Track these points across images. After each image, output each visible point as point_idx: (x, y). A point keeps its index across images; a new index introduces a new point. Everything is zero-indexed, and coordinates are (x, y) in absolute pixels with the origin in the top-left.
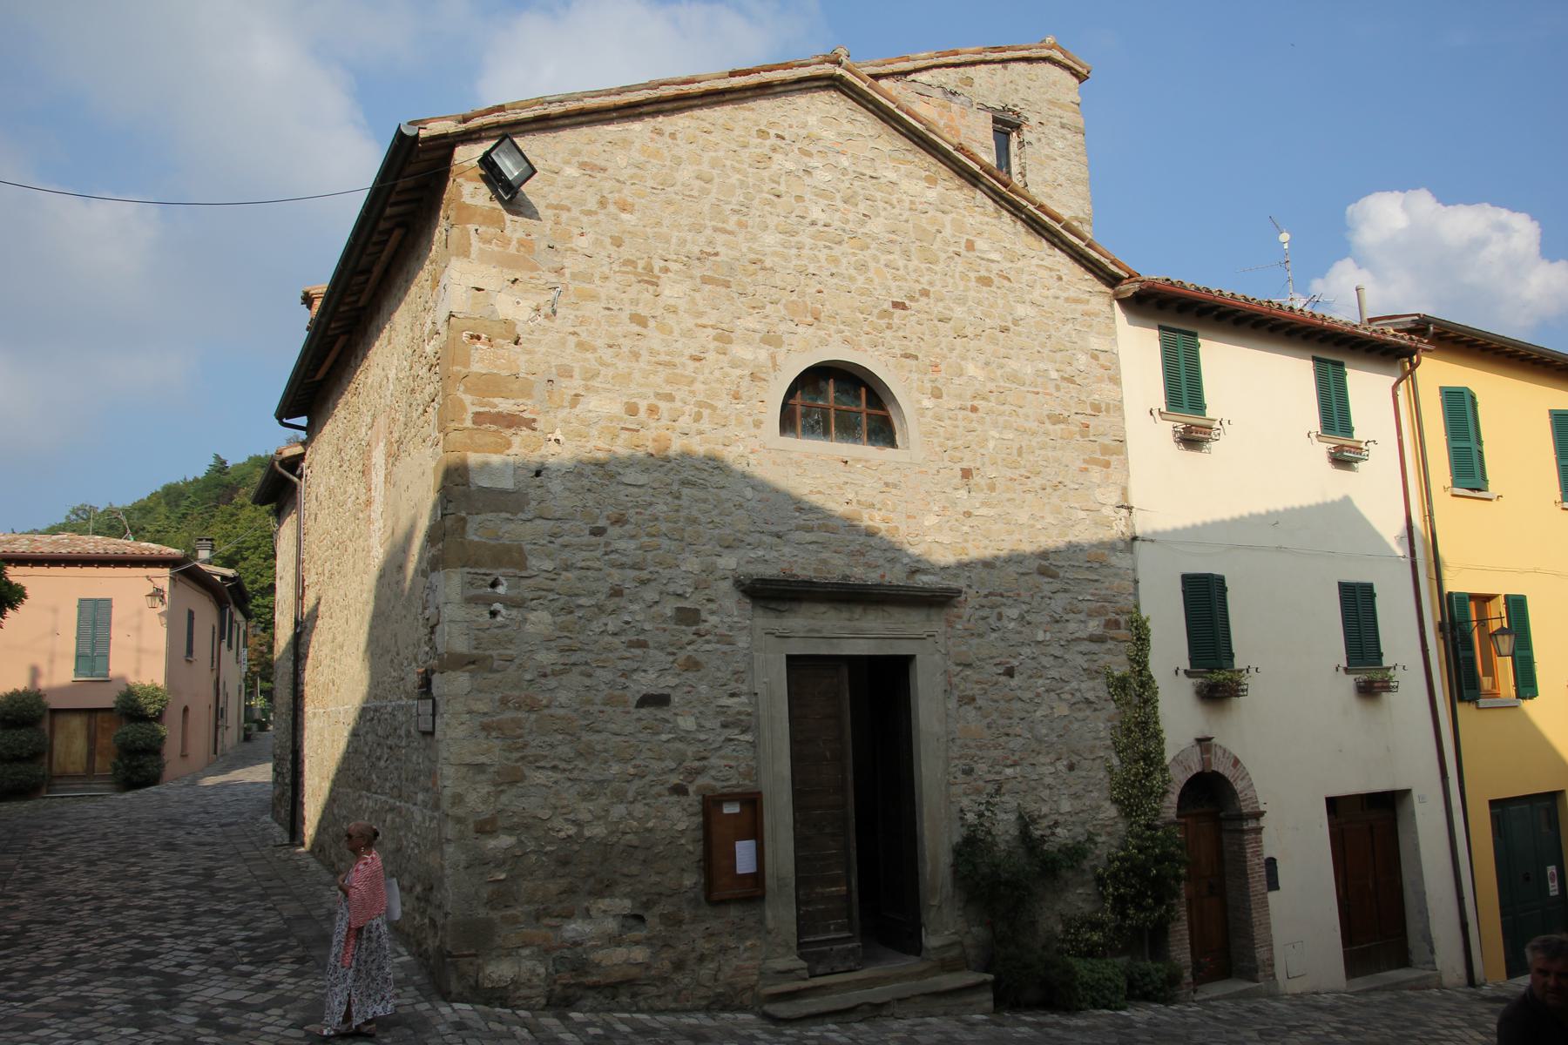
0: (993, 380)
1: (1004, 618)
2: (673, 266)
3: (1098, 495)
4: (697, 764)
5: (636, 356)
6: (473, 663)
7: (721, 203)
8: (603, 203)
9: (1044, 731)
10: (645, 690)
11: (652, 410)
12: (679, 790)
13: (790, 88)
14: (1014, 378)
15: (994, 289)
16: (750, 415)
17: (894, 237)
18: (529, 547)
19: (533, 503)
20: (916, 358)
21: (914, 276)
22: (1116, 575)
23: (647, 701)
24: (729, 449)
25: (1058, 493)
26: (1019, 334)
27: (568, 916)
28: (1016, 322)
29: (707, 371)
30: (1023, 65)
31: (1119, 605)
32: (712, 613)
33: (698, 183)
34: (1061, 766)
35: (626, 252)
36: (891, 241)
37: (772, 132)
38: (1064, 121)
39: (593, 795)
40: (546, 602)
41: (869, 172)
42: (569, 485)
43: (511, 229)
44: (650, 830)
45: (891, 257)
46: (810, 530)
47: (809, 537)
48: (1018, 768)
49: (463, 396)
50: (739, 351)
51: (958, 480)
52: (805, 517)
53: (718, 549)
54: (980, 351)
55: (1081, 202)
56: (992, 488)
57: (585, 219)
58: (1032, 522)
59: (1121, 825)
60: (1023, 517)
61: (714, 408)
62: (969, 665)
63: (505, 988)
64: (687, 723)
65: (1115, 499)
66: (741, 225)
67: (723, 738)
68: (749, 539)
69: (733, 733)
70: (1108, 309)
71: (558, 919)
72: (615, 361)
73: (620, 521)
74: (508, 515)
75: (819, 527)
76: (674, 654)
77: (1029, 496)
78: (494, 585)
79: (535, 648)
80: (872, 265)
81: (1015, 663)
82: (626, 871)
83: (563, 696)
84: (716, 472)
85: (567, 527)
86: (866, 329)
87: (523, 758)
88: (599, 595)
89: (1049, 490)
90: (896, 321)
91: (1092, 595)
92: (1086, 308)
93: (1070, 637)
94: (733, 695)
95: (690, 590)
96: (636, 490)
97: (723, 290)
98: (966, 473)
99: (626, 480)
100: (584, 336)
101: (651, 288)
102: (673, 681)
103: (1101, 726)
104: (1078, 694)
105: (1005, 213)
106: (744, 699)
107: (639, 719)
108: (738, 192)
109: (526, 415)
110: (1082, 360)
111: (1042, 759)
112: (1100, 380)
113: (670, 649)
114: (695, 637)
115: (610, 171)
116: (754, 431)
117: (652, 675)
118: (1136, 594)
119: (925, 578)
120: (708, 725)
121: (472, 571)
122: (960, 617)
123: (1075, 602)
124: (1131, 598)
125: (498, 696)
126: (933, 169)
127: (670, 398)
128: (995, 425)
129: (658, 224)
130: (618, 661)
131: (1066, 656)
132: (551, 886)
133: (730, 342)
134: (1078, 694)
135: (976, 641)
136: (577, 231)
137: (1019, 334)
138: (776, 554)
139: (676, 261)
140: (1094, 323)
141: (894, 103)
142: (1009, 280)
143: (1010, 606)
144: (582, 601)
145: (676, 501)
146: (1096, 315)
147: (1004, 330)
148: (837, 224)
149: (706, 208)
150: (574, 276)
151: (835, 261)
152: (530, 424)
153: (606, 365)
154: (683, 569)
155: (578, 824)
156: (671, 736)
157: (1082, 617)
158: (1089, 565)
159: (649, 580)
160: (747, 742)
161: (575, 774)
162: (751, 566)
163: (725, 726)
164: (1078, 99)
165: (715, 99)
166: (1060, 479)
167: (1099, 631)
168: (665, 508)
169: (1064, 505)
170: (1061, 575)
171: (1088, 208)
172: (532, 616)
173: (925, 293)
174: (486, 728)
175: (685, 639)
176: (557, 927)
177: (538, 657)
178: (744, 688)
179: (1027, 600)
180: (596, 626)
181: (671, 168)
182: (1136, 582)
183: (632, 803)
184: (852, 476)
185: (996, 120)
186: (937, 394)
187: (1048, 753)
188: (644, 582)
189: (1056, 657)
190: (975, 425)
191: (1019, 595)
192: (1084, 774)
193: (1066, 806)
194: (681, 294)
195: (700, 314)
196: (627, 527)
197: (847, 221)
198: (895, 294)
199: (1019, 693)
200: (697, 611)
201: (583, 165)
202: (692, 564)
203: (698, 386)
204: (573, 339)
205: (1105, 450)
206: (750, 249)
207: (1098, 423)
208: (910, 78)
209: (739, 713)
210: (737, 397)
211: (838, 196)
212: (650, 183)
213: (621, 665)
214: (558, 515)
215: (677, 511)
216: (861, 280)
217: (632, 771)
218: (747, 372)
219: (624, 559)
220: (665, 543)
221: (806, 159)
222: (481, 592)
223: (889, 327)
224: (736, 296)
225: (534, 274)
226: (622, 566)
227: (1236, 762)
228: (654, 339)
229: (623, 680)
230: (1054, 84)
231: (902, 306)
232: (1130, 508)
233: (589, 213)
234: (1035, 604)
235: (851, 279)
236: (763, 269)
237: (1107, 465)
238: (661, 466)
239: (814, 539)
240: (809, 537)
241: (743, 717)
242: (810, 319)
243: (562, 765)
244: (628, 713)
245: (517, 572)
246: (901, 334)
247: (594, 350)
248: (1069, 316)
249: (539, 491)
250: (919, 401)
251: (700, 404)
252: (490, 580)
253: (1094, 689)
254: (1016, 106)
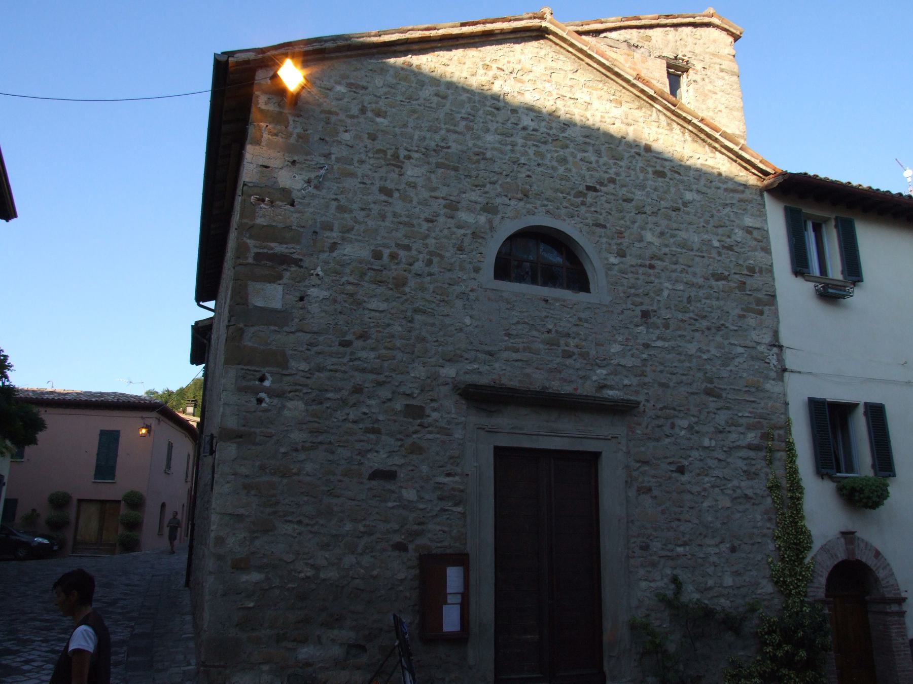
0: (666, 246)
3: (754, 335)
4: (416, 527)
5: (383, 217)
6: (241, 437)
7: (453, 113)
8: (363, 110)
9: (710, 519)
10: (376, 466)
11: (393, 256)
12: (401, 547)
13: (508, 37)
14: (684, 245)
15: (667, 179)
16: (470, 263)
17: (588, 140)
18: (291, 352)
19: (296, 320)
20: (604, 227)
21: (604, 168)
22: (770, 398)
23: (377, 475)
24: (454, 287)
25: (721, 333)
26: (688, 213)
27: (304, 641)
28: (685, 204)
29: (437, 230)
30: (690, 29)
31: (773, 422)
32: (435, 410)
33: (435, 99)
34: (725, 547)
35: (378, 145)
36: (585, 143)
37: (494, 66)
38: (723, 67)
40: (301, 395)
41: (569, 95)
42: (326, 308)
43: (292, 126)
44: (375, 577)
45: (585, 155)
46: (517, 351)
47: (515, 356)
48: (687, 548)
49: (248, 241)
50: (463, 216)
51: (637, 320)
52: (512, 341)
53: (441, 361)
54: (656, 224)
55: (737, 123)
56: (667, 326)
57: (349, 121)
58: (699, 354)
59: (776, 601)
60: (692, 348)
61: (442, 257)
62: (646, 463)
64: (410, 494)
65: (767, 339)
66: (469, 128)
67: (438, 508)
68: (466, 355)
69: (448, 505)
70: (759, 198)
72: (366, 220)
73: (363, 336)
74: (276, 328)
75: (525, 349)
76: (401, 440)
77: (697, 335)
78: (262, 379)
80: (570, 159)
81: (686, 463)
83: (309, 467)
84: (442, 304)
85: (321, 339)
86: (565, 204)
87: (275, 513)
88: (344, 391)
89: (714, 331)
90: (589, 200)
91: (750, 412)
92: (742, 196)
93: (731, 445)
94: (449, 475)
95: (417, 392)
96: (378, 314)
97: (453, 173)
98: (645, 314)
99: (370, 306)
100: (343, 202)
101: (397, 170)
102: (397, 460)
103: (759, 517)
104: (739, 491)
105: (675, 126)
106: (457, 478)
107: (370, 489)
108: (468, 105)
109: (295, 256)
110: (739, 235)
111: (708, 541)
112: (754, 249)
113: (399, 436)
114: (419, 428)
115: (370, 89)
116: (473, 275)
117: (383, 455)
118: (786, 413)
119: (611, 393)
120: (427, 497)
121: (245, 367)
122: (640, 424)
123: (736, 417)
124: (782, 416)
125: (258, 463)
126: (618, 94)
127: (408, 248)
128: (669, 279)
129: (405, 126)
131: (729, 460)
133: (457, 209)
134: (739, 491)
135: (652, 444)
136: (342, 129)
137: (688, 213)
138: (488, 368)
139: (417, 151)
140: (749, 207)
141: (586, 46)
142: (679, 174)
143: (682, 418)
144: (330, 395)
145: (409, 324)
146: (750, 202)
147: (677, 210)
148: (543, 129)
149: (442, 116)
150: (338, 160)
151: (542, 155)
152: (297, 263)
153: (360, 223)
154: (413, 375)
156: (395, 504)
157: (741, 429)
158: (747, 389)
159: (384, 382)
160: (459, 513)
161: (316, 528)
162: (468, 376)
163: (441, 499)
164: (733, 52)
165: (451, 43)
166: (722, 322)
167: (756, 442)
168: (400, 329)
169: (726, 342)
170: (724, 395)
171: (742, 128)
172: (290, 404)
173: (612, 181)
174: (246, 487)
175: (411, 429)
177: (292, 436)
178: (459, 470)
179: (696, 414)
180: (340, 415)
181: (416, 88)
182: (787, 404)
183: (361, 554)
184: (551, 311)
185: (669, 66)
186: (621, 254)
187: (713, 537)
189: (720, 460)
190: (652, 278)
191: (688, 409)
192: (744, 555)
193: (728, 581)
194: (420, 174)
195: (435, 189)
196: (369, 341)
197: (551, 128)
198: (588, 180)
199: (688, 487)
200: (422, 409)
201: (349, 85)
202: (419, 371)
203: (431, 241)
204: (334, 204)
205: (759, 302)
206: (474, 145)
207: (755, 282)
208: (602, 35)
209: (453, 489)
210: (461, 249)
212: (399, 98)
213: (359, 446)
214: (315, 329)
215: (410, 331)
216: (561, 170)
217: (362, 529)
218: (469, 232)
219: (365, 365)
220: (399, 355)
221: (519, 85)
222: (251, 383)
223: (583, 203)
224: (462, 177)
225: (309, 158)
226: (363, 371)
228: (399, 206)
229: (359, 457)
230: (714, 41)
231: (595, 189)
232: (781, 347)
233: (353, 117)
234: (702, 417)
235: (554, 169)
236: (483, 159)
237: (761, 313)
238: (399, 298)
239: (519, 357)
240: (515, 356)
241: (457, 493)
242: (520, 196)
243: (306, 521)
244: (361, 483)
245: (280, 370)
246: (593, 209)
247: (351, 211)
248: (728, 202)
249: (301, 312)
250: (607, 259)
251: (431, 253)
252: (258, 375)
253: (752, 487)
254: (684, 56)
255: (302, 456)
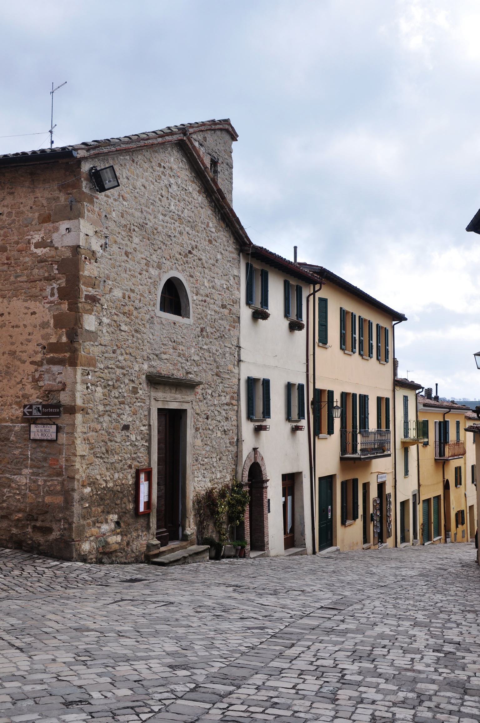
1: (208, 395)
2: (136, 229)
12: (130, 467)
32: (141, 389)
39: (109, 469)
44: (123, 484)
52: (164, 347)
63: (86, 554)
71: (100, 524)
78: (88, 374)
79: (98, 404)
82: (117, 502)
91: (228, 385)
109: (98, 297)
121: (83, 368)
127: (132, 291)
130: (118, 410)
132: (99, 509)
155: (106, 481)
157: (225, 394)
158: (228, 372)
161: (106, 460)
162: (150, 369)
176: (100, 527)
188: (124, 375)
189: (218, 411)
192: (223, 462)
211: (177, 197)
217: (120, 458)
227: (262, 458)
238: (131, 322)
249: (101, 332)
255: (101, 419)
